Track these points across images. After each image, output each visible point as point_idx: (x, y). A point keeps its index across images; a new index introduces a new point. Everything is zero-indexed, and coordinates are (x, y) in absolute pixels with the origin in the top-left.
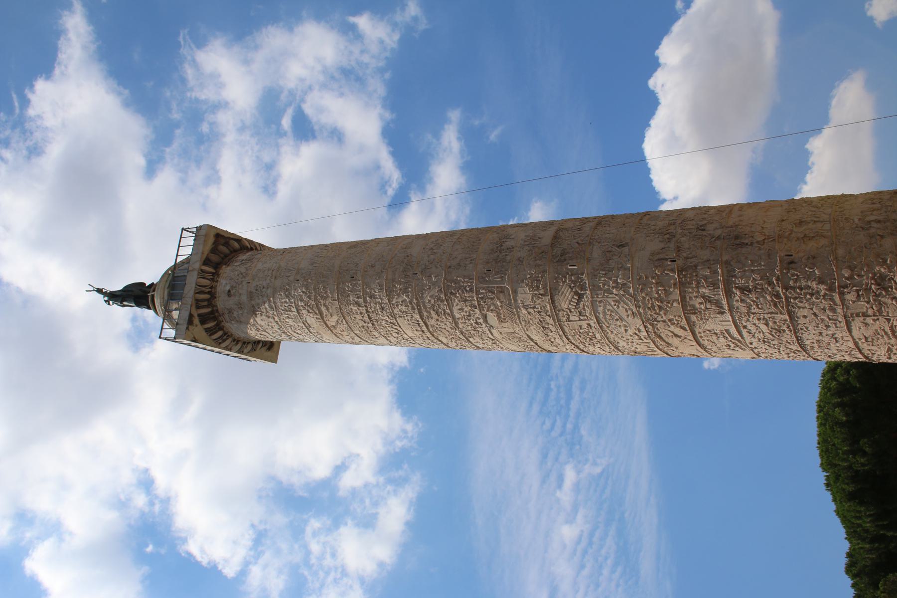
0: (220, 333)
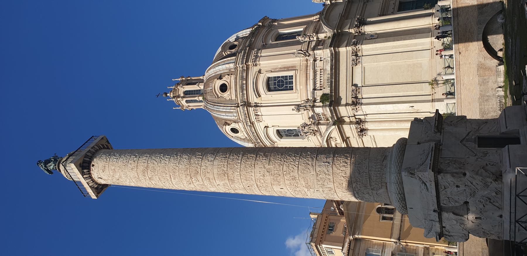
0: (102, 147)
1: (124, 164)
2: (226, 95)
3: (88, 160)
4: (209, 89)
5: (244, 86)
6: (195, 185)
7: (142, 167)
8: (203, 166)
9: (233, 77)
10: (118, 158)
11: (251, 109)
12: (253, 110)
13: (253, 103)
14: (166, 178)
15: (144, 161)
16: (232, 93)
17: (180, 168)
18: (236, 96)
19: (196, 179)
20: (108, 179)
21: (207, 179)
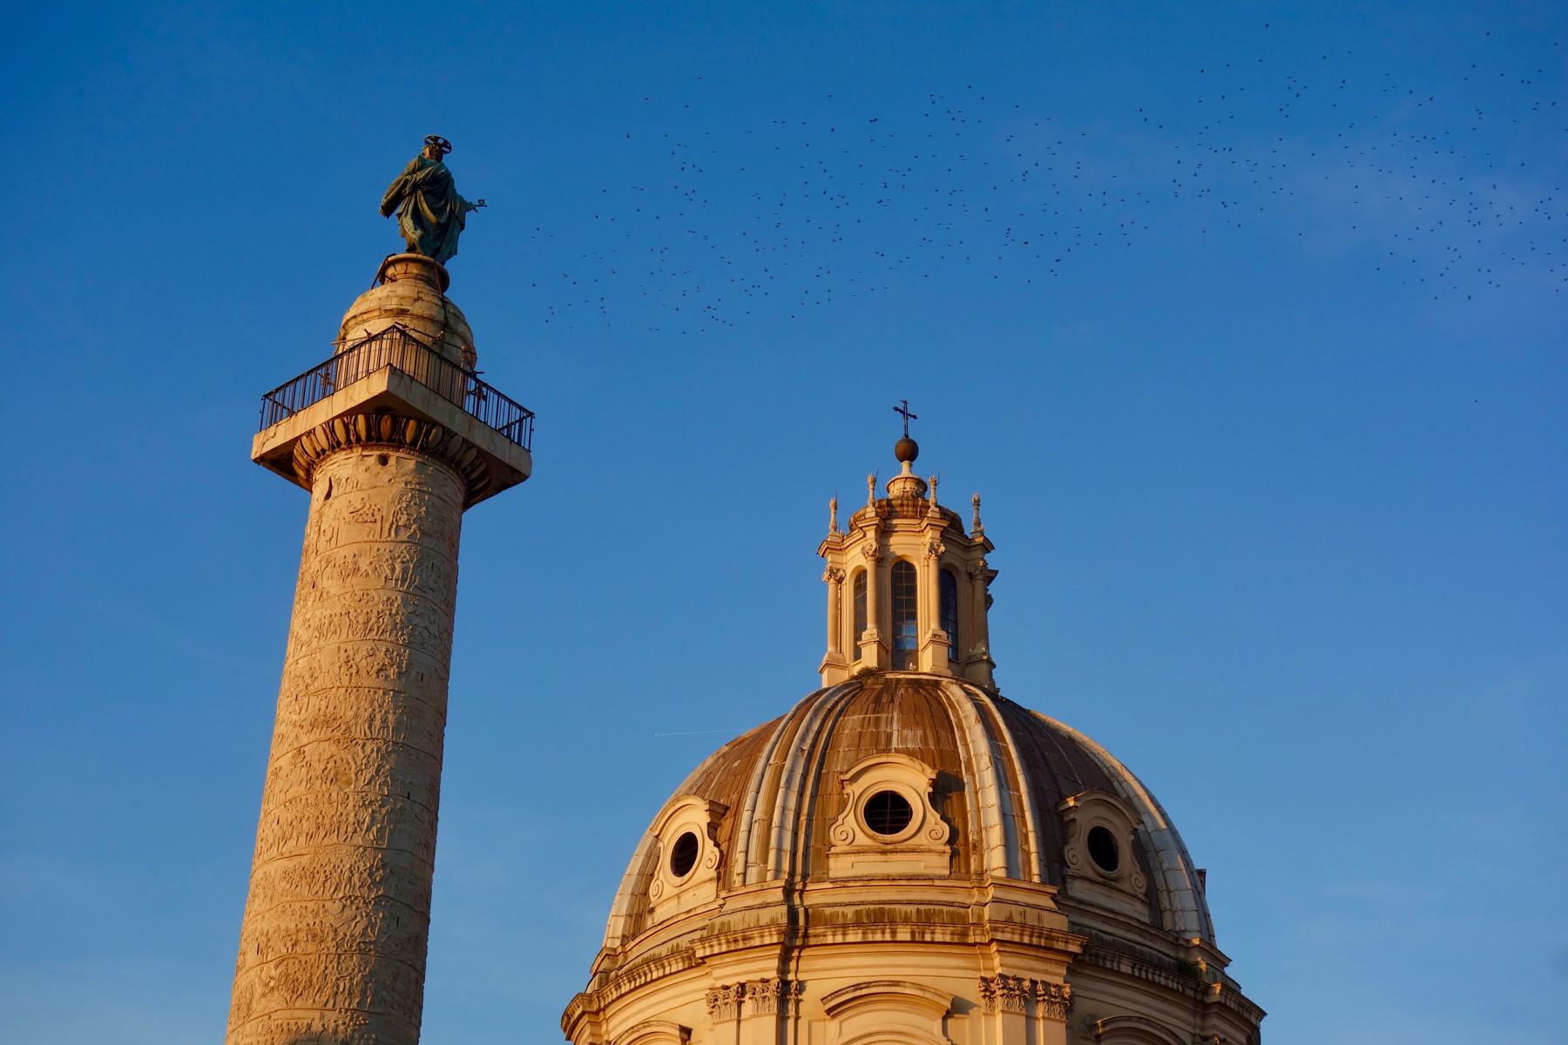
0: (474, 476)
1: (374, 619)
2: (850, 827)
3: (409, 435)
4: (895, 726)
5: (883, 933)
6: (252, 973)
7: (350, 714)
8: (326, 1020)
9: (938, 864)
10: (404, 580)
11: (766, 967)
12: (766, 976)
13: (801, 977)
14: (295, 835)
15: (377, 722)
16: (861, 857)
17: (329, 905)
18: (842, 882)
19: (272, 984)
20: (322, 531)
21: (269, 1037)
